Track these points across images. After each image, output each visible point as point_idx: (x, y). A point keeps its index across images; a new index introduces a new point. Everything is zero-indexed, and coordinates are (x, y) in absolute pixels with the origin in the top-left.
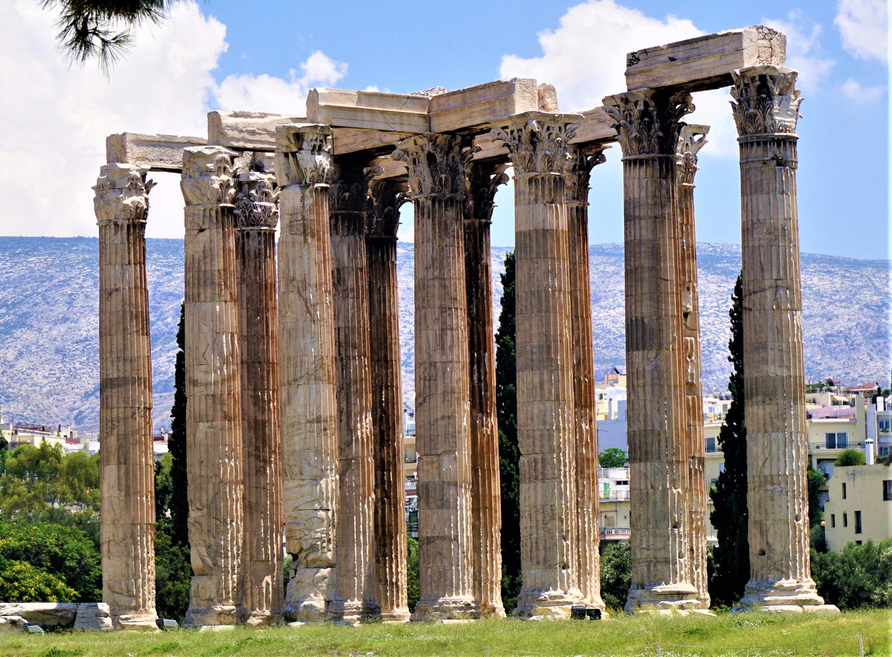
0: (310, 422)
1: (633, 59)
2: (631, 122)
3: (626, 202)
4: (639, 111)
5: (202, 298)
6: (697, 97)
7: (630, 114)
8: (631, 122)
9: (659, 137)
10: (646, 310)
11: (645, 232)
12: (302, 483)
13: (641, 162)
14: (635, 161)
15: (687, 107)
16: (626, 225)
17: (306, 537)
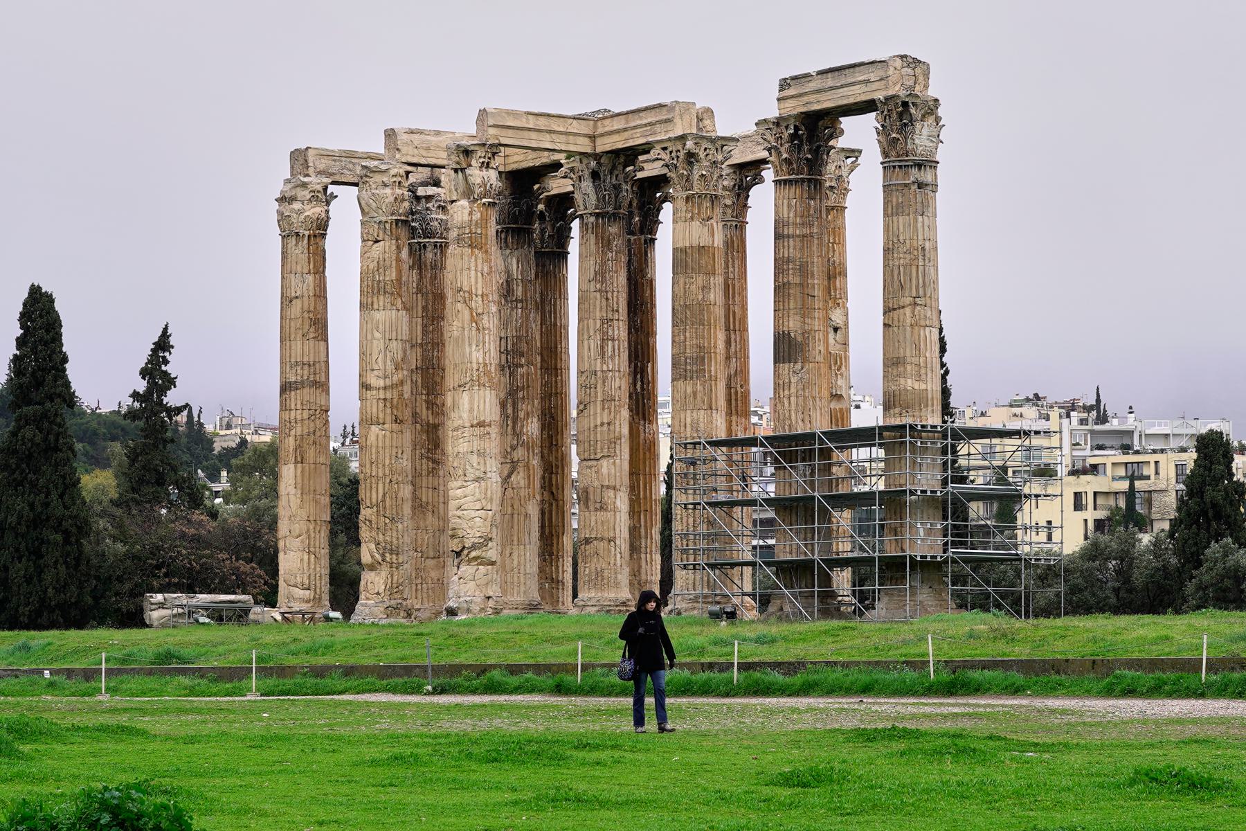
0: (472, 426)
1: (785, 84)
2: (781, 145)
3: (776, 221)
4: (790, 134)
5: (376, 306)
6: (846, 122)
7: (781, 137)
8: (781, 145)
9: (807, 159)
10: (793, 324)
11: (792, 250)
12: (465, 484)
13: (790, 181)
14: (785, 181)
15: (836, 133)
16: (775, 243)
17: (468, 536)
